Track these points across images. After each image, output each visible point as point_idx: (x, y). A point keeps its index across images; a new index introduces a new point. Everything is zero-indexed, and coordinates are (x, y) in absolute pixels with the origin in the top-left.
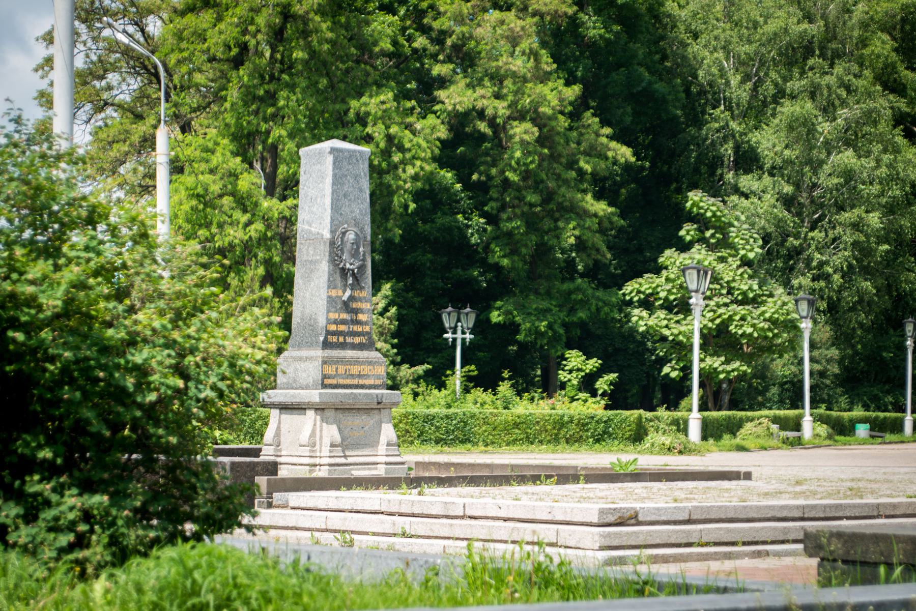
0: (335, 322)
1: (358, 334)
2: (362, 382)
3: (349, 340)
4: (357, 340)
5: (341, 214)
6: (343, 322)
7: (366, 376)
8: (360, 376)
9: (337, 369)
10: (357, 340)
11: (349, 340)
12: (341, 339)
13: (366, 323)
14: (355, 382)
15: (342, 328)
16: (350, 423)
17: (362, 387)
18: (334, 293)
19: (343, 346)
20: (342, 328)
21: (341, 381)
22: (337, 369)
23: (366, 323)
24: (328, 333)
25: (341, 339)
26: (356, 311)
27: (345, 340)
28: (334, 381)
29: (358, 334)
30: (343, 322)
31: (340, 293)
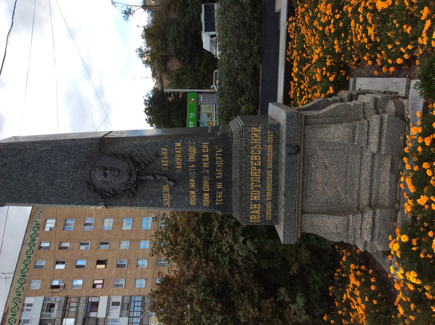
0: (200, 195)
1: (212, 160)
2: (270, 165)
3: (219, 175)
4: (220, 162)
5: (73, 189)
6: (199, 183)
7: (263, 155)
8: (263, 167)
9: (255, 202)
10: (220, 162)
11: (219, 175)
12: (219, 186)
13: (199, 148)
14: (269, 174)
15: (206, 185)
16: (319, 187)
17: (276, 162)
18: (167, 198)
19: (227, 181)
20: (206, 185)
21: (269, 195)
22: (255, 202)
23: (199, 148)
25: (219, 186)
26: (186, 163)
27: (219, 180)
28: (269, 206)
30: (199, 183)
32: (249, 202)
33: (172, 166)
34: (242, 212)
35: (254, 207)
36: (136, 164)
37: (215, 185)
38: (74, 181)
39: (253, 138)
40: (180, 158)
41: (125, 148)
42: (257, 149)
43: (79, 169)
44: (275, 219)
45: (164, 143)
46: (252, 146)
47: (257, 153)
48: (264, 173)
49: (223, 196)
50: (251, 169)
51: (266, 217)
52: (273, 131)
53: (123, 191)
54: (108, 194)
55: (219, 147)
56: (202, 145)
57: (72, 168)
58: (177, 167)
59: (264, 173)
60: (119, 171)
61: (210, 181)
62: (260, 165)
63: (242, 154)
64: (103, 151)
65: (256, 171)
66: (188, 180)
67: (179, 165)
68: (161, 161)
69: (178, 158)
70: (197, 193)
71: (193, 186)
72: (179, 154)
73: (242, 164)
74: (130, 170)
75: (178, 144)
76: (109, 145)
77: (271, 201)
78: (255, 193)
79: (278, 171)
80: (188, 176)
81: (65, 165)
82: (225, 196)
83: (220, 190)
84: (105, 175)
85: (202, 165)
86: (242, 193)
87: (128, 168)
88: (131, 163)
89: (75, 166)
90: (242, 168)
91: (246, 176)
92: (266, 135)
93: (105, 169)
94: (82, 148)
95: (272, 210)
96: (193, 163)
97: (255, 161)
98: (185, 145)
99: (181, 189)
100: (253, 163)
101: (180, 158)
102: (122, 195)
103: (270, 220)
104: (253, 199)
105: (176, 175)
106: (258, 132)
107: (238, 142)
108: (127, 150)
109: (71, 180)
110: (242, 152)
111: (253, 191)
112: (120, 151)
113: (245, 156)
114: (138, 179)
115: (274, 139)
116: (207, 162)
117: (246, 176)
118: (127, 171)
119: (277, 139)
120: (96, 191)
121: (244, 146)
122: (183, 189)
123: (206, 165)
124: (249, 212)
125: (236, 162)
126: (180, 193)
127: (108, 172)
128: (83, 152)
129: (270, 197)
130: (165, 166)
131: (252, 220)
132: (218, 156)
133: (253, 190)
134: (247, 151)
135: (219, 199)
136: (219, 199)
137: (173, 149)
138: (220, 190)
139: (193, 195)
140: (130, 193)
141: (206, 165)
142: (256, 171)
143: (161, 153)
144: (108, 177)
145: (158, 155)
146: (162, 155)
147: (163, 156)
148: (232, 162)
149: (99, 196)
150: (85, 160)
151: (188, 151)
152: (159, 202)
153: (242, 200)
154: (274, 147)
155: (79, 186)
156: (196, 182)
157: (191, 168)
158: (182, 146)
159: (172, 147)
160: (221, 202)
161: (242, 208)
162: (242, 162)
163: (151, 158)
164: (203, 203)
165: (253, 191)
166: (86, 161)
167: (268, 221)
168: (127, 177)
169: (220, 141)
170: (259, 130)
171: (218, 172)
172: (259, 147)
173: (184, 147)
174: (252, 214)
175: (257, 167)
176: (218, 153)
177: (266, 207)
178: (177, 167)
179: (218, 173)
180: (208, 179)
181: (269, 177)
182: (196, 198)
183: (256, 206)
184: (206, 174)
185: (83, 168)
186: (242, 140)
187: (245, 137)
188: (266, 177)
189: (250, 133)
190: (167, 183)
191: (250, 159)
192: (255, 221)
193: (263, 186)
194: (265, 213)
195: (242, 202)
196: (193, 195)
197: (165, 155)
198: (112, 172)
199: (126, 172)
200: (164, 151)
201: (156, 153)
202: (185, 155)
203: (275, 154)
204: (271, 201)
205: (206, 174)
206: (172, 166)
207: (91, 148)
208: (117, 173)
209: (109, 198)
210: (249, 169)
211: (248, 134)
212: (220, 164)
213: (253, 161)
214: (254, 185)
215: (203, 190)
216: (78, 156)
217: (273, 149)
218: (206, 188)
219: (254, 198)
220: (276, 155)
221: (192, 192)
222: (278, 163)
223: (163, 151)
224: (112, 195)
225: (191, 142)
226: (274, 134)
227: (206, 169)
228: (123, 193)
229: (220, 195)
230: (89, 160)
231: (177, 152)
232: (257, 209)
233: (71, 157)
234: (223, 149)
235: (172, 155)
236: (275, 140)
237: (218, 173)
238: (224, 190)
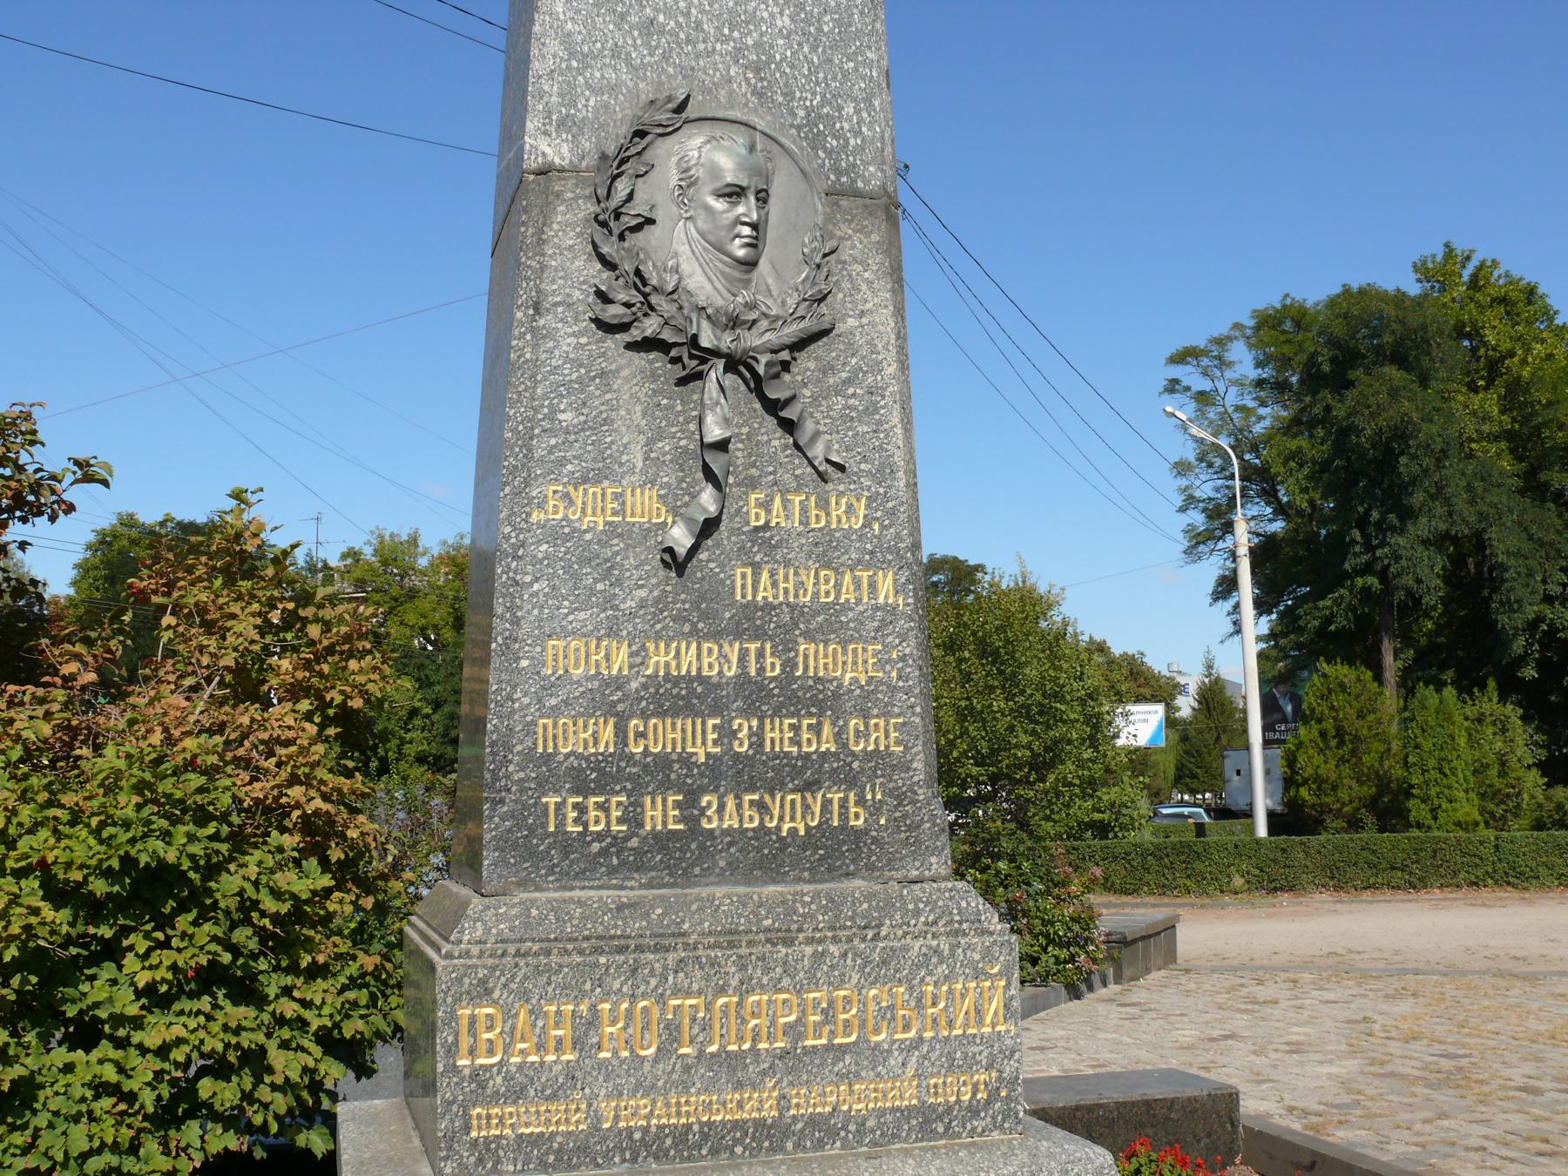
0: (607, 699)
1: (804, 774)
2: (809, 1101)
3: (726, 814)
4: (791, 815)
8: (794, 1062)
10: (791, 815)
11: (726, 814)
12: (661, 814)
13: (867, 700)
14: (761, 1104)
20: (665, 736)
24: (549, 772)
27: (690, 808)
29: (804, 774)
31: (645, 506)
32: (584, 994)
33: (764, 544)
34: (518, 954)
35: (557, 1026)
36: (785, 355)
37: (666, 786)
38: (688, 41)
39: (950, 991)
40: (816, 594)
41: (862, 314)
42: (893, 1018)
43: (757, 70)
44: (480, 1161)
45: (892, 513)
46: (911, 989)
47: (871, 1023)
48: (764, 1073)
49: (599, 836)
50: (780, 991)
51: (495, 1098)
52: (988, 1102)
53: (638, 273)
54: (622, 188)
55: (875, 809)
56: (886, 715)
57: (758, 45)
58: (765, 576)
59: (764, 1073)
60: (750, 264)
61: (686, 760)
62: (808, 1043)
63: (864, 939)
64: (844, 203)
65: (773, 1023)
66: (695, 631)
67: (775, 584)
68: (797, 491)
69: (813, 586)
70: (618, 683)
71: (659, 659)
72: (838, 593)
73: (810, 941)
74: (754, 322)
75: (886, 584)
76: (875, 238)
77: (596, 1127)
78: (646, 1027)
79: (772, 1150)
80: (716, 636)
81: (772, 15)
82: (596, 847)
83: (633, 818)
84: (734, 193)
85: (777, 712)
86: (640, 949)
87: (766, 316)
88: (792, 331)
89: (771, 59)
90: (789, 942)
91: (743, 968)
92: (970, 1064)
93: (763, 197)
94: (858, 111)
95: (536, 1140)
96: (789, 665)
97: (828, 1014)
98: (883, 624)
99: (643, 593)
100: (816, 1002)
101: (816, 594)
102: (609, 264)
103: (467, 1128)
104: (606, 1018)
105: (722, 566)
106: (981, 1023)
107: (917, 913)
108: (851, 322)
109: (698, 25)
110: (876, 937)
111: (656, 1013)
112: (846, 285)
113: (856, 955)
114: (706, 355)
115: (950, 1109)
116: (796, 741)
117: (743, 968)
118: (751, 306)
119: (948, 1127)
120: (640, 134)
121: (906, 949)
122: (642, 604)
123: (778, 735)
124: (525, 996)
125: (804, 904)
126: (618, 582)
127: (747, 209)
128: (840, 109)
129: (617, 1118)
130: (769, 511)
131: (473, 1020)
132: (827, 804)
133: (663, 1011)
134: (884, 968)
135: (581, 809)
136: (581, 809)
137: (859, 561)
138: (633, 818)
139: (607, 657)
140: (628, 305)
141: (778, 735)
142: (773, 1023)
143: (841, 494)
144: (719, 205)
145: (829, 472)
146: (827, 502)
147: (824, 504)
148: (799, 880)
149: (611, 150)
150: (802, 113)
151: (852, 640)
152: (562, 462)
153: (598, 951)
154: (906, 1113)
155: (666, 57)
156: (679, 678)
157: (760, 654)
158: (877, 608)
159: (872, 553)
160: (561, 823)
161: (548, 953)
162: (820, 941)
163: (816, 435)
164: (555, 712)
165: (656, 1013)
166: (795, 115)
167: (467, 1118)
168: (720, 302)
169: (905, 816)
170: (993, 1025)
171: (739, 807)
172: (907, 1028)
173: (873, 618)
174: (509, 1015)
175: (795, 1031)
176: (844, 804)
177: (553, 1097)
178: (765, 576)
179: (730, 803)
180: (701, 752)
181: (740, 1105)
182: (589, 679)
183: (559, 1041)
184: (727, 734)
185: (759, 94)
186: (934, 936)
187: (953, 948)
188: (739, 1086)
189: (978, 975)
190: (675, 511)
191: (842, 982)
192: (465, 1042)
193: (687, 1069)
194: (516, 1094)
195: (581, 952)
196: (607, 657)
197: (828, 514)
198: (746, 231)
199: (740, 299)
200: (846, 511)
201: (841, 468)
202: (830, 623)
203: (871, 1123)
204: (596, 1127)
205: (727, 734)
206: (770, 548)
207: (861, 149)
208: (741, 253)
209: (602, 192)
210: (786, 982)
211: (973, 965)
212: (781, 819)
213: (831, 1003)
214: (694, 1019)
215: (630, 717)
216: (817, 83)
217: (894, 1110)
218: (643, 735)
219: (613, 1023)
220: (861, 1131)
221: (621, 657)
222: (819, 1145)
223: (850, 506)
224: (617, 215)
225: (903, 659)
226: (973, 1111)
227: (757, 738)
228: (628, 267)
229: (604, 816)
230: (799, 128)
231: (847, 578)
232: (541, 1047)
233: (814, 49)
234: (866, 832)
235: (827, 550)
236: (940, 1118)
237: (730, 803)
238: (634, 843)
